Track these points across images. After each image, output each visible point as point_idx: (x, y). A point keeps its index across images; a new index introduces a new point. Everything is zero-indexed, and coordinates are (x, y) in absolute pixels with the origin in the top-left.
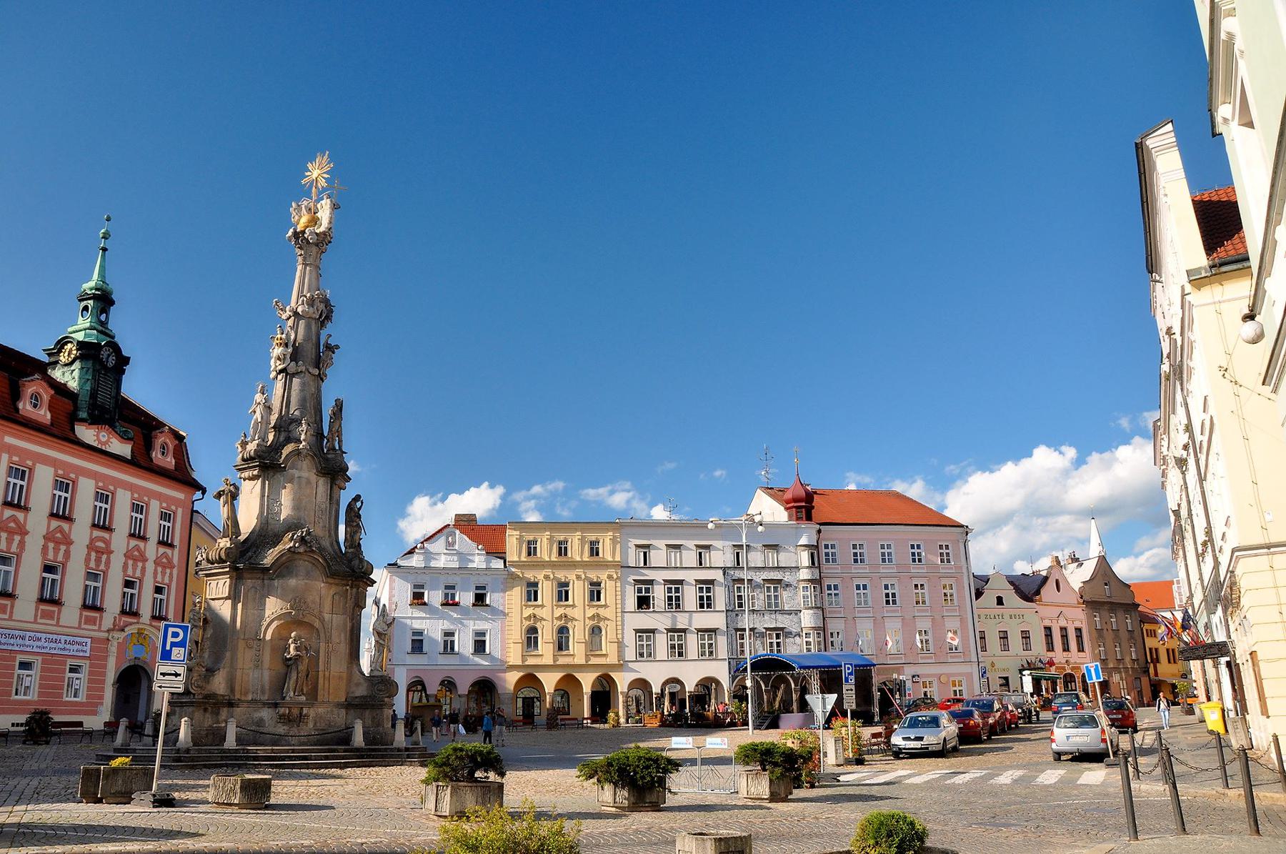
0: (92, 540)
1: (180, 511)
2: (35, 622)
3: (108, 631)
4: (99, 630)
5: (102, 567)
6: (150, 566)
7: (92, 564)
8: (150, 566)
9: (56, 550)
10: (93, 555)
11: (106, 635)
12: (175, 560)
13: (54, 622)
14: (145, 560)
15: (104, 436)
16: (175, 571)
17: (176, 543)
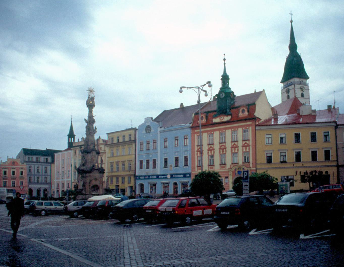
0: (221, 146)
1: (250, 128)
2: (220, 169)
3: (228, 169)
4: (226, 169)
5: (224, 153)
6: (240, 148)
7: (221, 153)
8: (240, 148)
9: (211, 152)
10: (221, 150)
11: (228, 170)
12: (251, 143)
13: (225, 169)
14: (238, 147)
15: (222, 117)
16: (251, 147)
17: (251, 138)
